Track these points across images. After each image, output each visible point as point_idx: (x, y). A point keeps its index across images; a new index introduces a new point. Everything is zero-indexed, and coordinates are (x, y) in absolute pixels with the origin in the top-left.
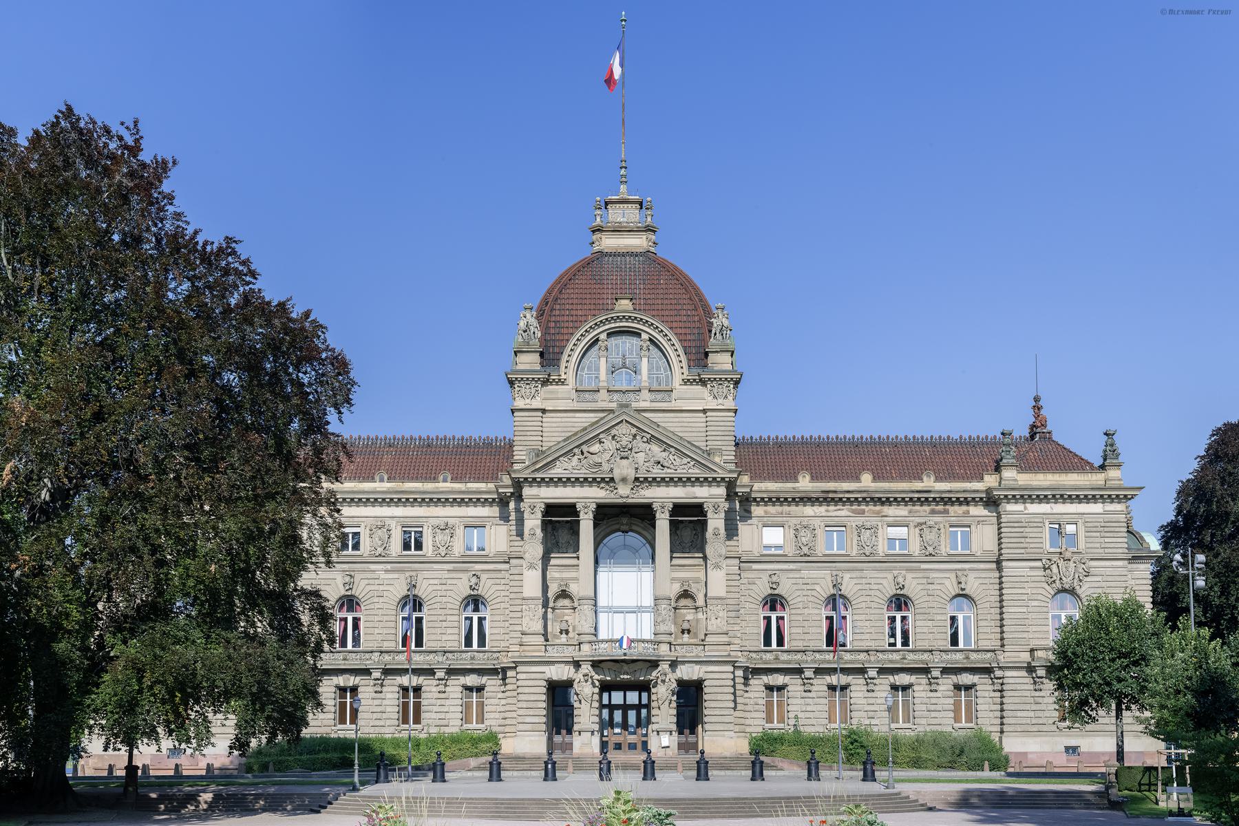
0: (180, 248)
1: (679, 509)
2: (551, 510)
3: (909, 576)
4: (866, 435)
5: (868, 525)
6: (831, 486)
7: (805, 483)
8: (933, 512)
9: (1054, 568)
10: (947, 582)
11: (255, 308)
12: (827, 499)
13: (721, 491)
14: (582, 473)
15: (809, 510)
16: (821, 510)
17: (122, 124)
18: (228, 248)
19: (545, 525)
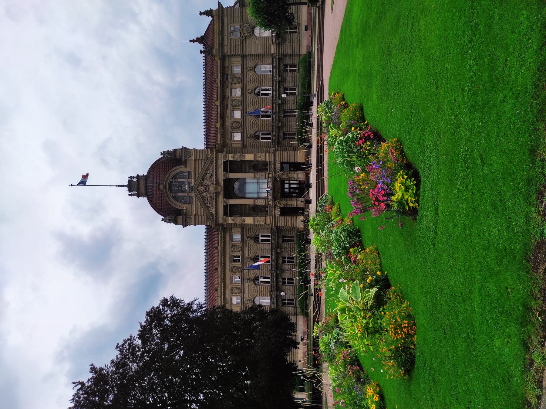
0: (119, 365)
1: (226, 170)
2: (226, 214)
3: (248, 88)
4: (203, 103)
5: (231, 103)
6: (219, 116)
7: (219, 125)
8: (227, 79)
9: (246, 35)
10: (250, 74)
11: (144, 334)
12: (223, 117)
13: (220, 155)
14: (214, 204)
15: (227, 124)
16: (227, 119)
17: (73, 389)
18: (120, 348)
19: (231, 216)
